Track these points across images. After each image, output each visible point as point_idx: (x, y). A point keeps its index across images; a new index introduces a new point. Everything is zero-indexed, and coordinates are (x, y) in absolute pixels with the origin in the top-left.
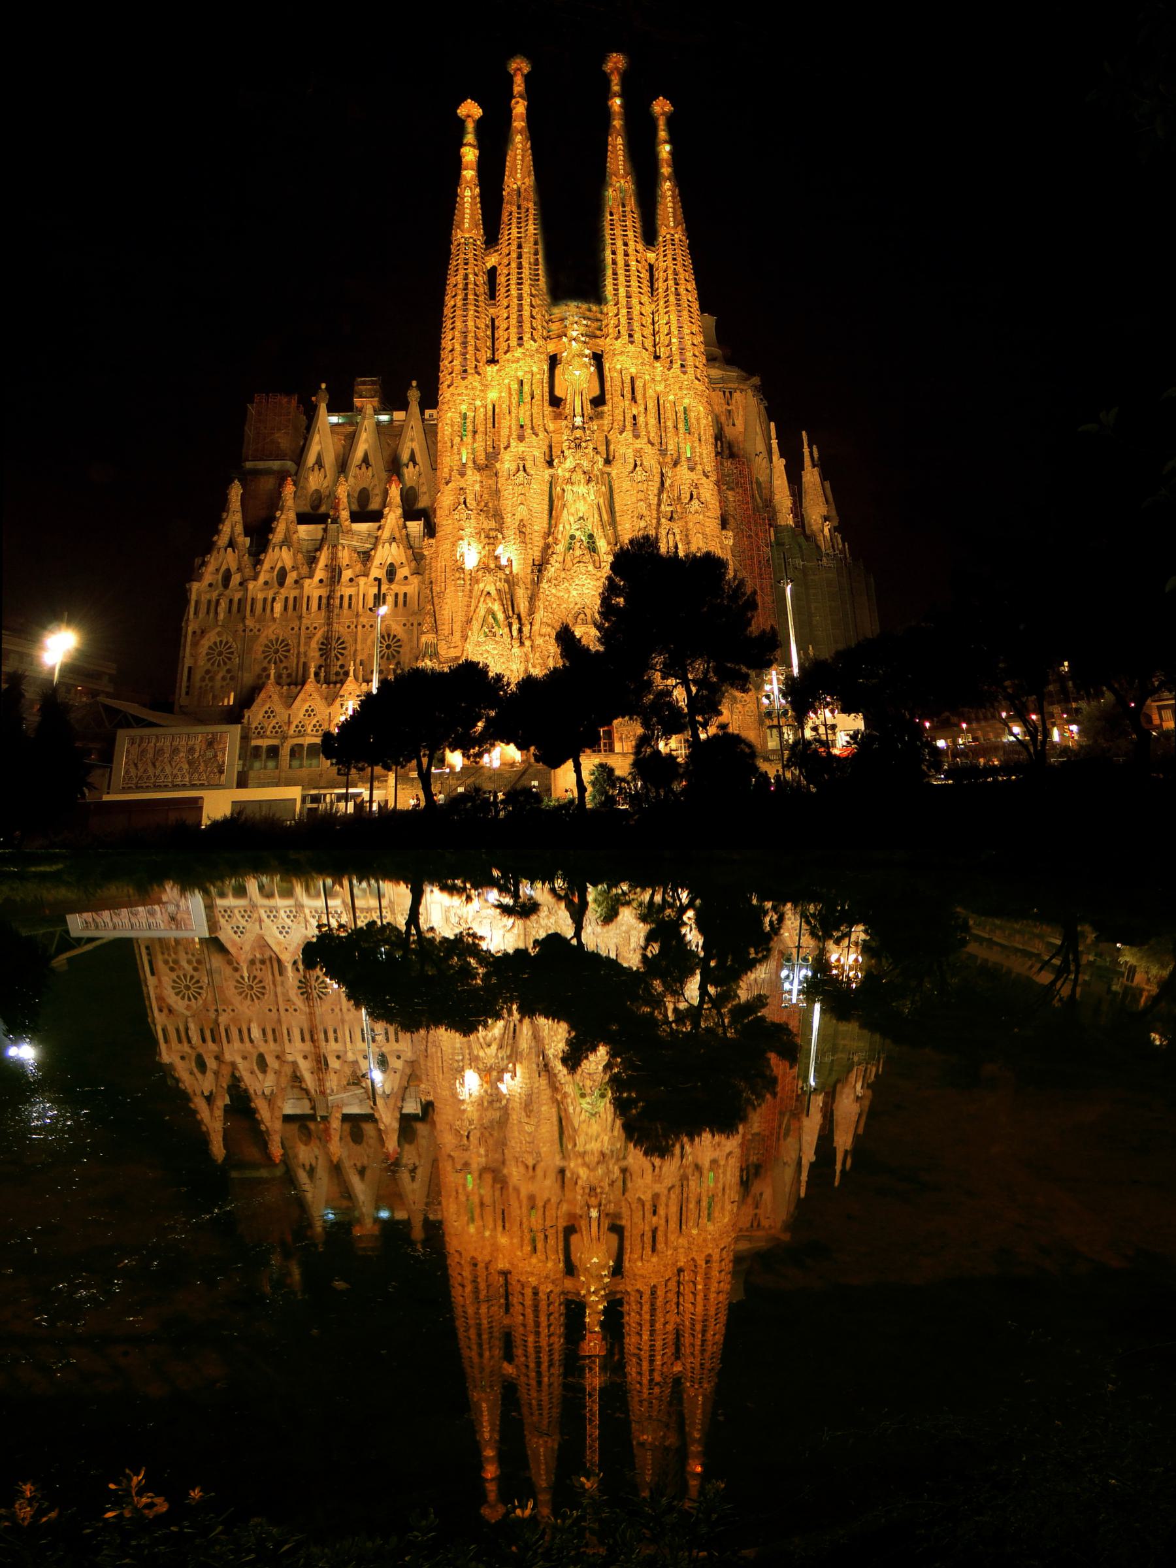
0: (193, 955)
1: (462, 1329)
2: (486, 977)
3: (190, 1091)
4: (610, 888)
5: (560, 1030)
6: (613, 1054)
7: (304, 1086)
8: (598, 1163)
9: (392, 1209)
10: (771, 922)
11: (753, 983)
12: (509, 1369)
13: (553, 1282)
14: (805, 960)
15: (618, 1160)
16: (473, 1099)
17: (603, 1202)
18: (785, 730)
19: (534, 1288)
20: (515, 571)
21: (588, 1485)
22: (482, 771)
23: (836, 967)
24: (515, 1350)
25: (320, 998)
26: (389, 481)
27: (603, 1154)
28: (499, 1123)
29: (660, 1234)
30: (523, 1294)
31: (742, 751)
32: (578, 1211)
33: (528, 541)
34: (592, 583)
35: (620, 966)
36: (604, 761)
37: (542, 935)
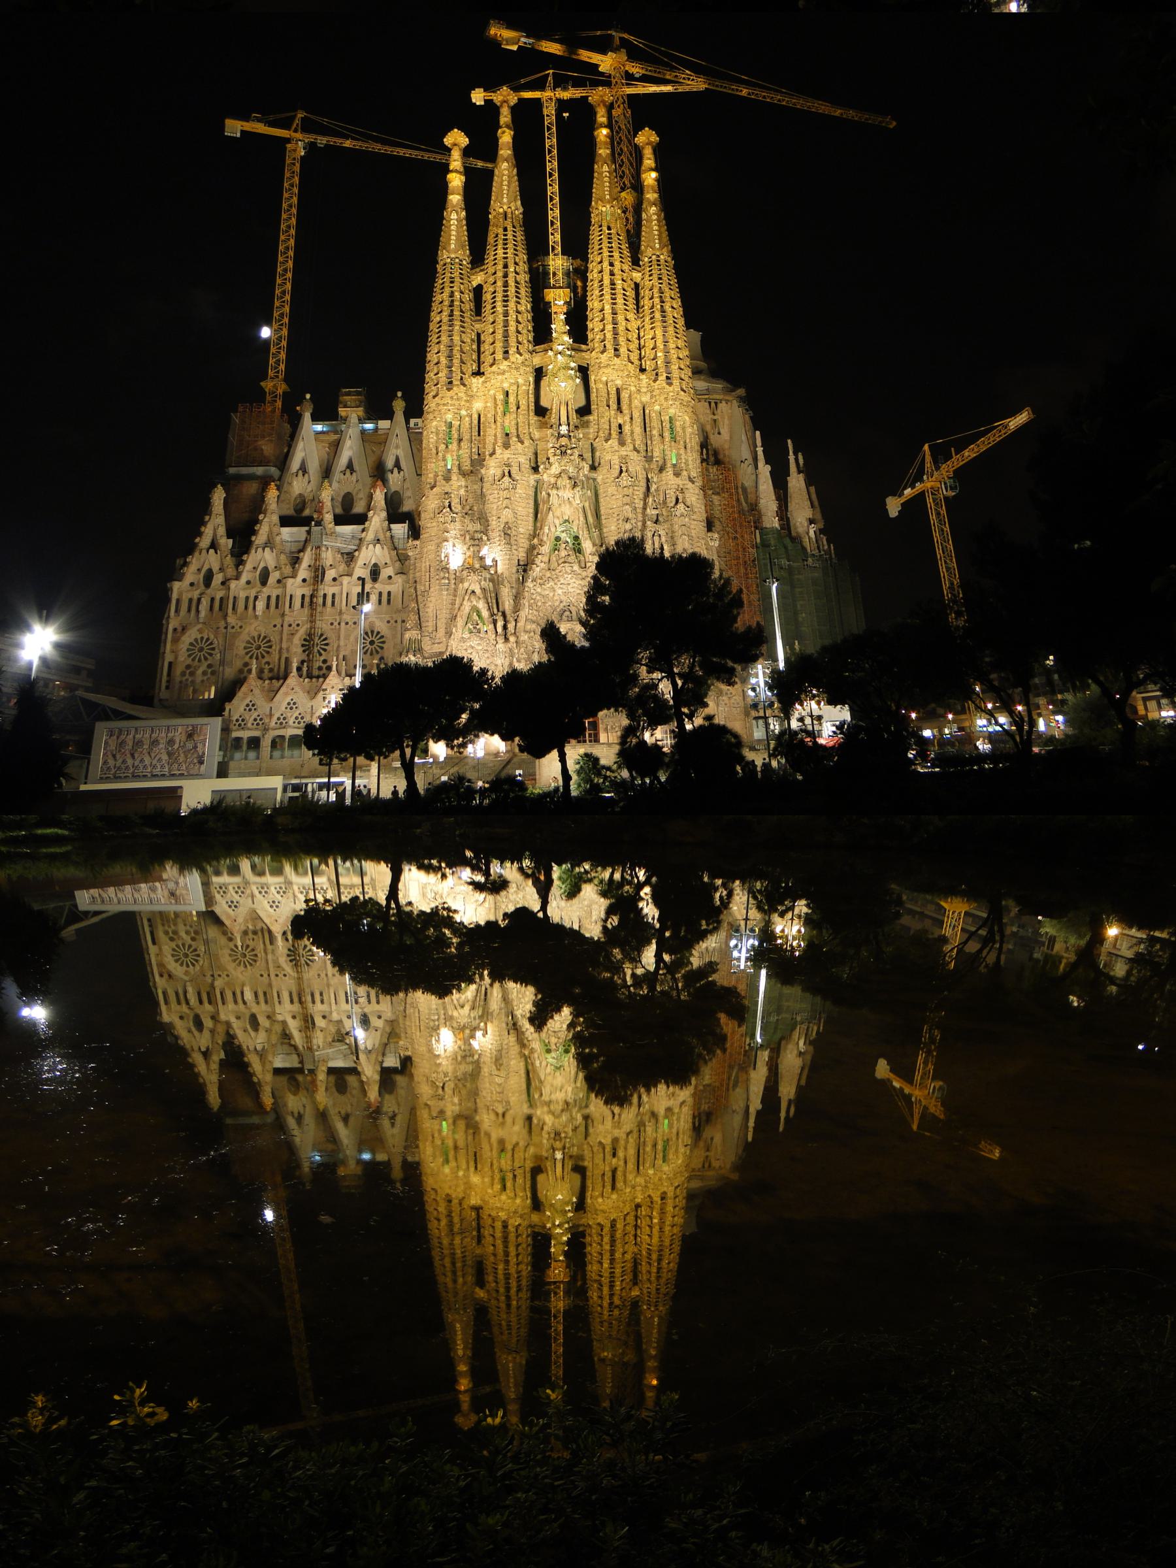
0: (191, 926)
1: (437, 1258)
2: (460, 946)
3: (188, 1047)
4: (573, 867)
5: (528, 993)
6: (576, 1014)
7: (293, 1043)
8: (563, 1111)
9: (373, 1152)
10: (721, 897)
11: (704, 951)
12: (481, 1294)
13: (521, 1217)
14: (752, 931)
15: (581, 1108)
16: (448, 1054)
17: (567, 1145)
18: (771, 721)
19: (504, 1222)
20: (500, 570)
21: (553, 1396)
22: (466, 760)
23: (781, 937)
24: (486, 1276)
25: (308, 965)
26: (374, 486)
27: (567, 1103)
28: (471, 1075)
29: (619, 1174)
30: (493, 1227)
31: (728, 742)
32: (545, 1154)
33: (513, 542)
34: (577, 582)
35: (583, 936)
36: (589, 751)
37: (511, 909)
